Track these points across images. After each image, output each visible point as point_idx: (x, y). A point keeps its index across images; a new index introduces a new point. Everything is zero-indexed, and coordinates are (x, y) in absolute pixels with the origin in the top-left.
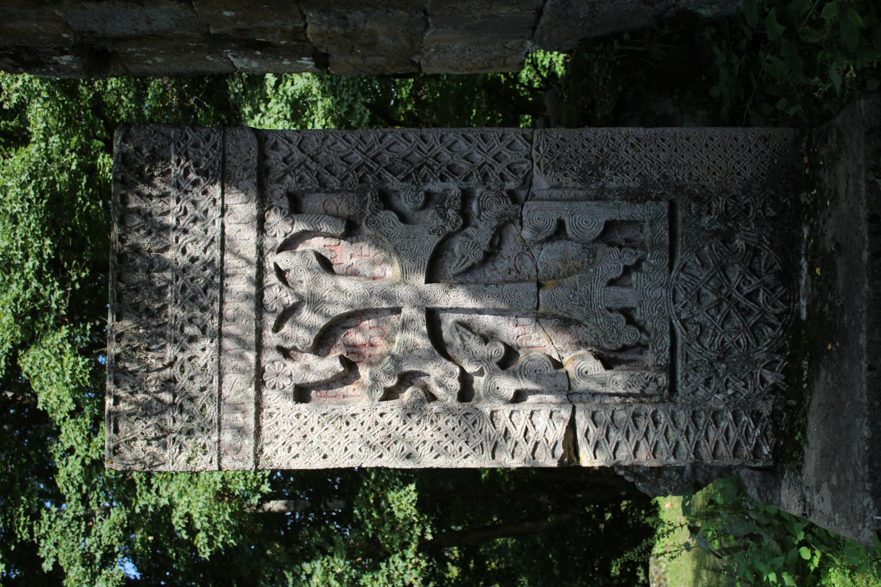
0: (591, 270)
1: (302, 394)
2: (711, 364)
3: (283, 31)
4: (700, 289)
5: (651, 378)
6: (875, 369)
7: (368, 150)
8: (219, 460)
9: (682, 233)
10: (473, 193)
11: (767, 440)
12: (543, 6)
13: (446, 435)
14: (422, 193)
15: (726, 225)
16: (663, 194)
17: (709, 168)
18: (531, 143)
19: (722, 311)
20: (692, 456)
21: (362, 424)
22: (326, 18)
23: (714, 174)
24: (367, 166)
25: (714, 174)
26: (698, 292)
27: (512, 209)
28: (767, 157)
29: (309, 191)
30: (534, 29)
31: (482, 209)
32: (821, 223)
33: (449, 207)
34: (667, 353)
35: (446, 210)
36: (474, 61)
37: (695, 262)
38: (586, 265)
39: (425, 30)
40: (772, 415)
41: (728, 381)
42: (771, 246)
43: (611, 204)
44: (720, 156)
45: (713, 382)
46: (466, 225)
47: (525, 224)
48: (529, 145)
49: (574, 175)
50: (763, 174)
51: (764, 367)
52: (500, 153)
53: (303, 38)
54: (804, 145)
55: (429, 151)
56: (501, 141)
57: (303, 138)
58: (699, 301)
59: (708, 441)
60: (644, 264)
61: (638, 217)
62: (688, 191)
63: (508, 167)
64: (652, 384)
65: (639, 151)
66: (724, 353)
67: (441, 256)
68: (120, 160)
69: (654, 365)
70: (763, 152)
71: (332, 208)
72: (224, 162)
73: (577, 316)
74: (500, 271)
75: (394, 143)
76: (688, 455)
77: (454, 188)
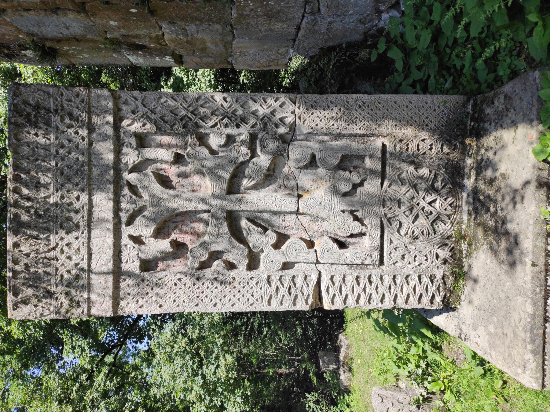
3: (150, 38)
6: (537, 265)
7: (189, 107)
11: (439, 293)
12: (301, 23)
13: (239, 291)
14: (224, 135)
17: (408, 122)
21: (185, 285)
22: (173, 28)
24: (188, 117)
28: (445, 114)
30: (294, 40)
39: (233, 40)
41: (416, 256)
44: (415, 114)
48: (294, 105)
50: (442, 126)
53: (163, 43)
54: (470, 107)
55: (229, 108)
57: (145, 97)
64: (369, 258)
68: (12, 108)
70: (443, 111)
73: (322, 215)
76: (390, 302)
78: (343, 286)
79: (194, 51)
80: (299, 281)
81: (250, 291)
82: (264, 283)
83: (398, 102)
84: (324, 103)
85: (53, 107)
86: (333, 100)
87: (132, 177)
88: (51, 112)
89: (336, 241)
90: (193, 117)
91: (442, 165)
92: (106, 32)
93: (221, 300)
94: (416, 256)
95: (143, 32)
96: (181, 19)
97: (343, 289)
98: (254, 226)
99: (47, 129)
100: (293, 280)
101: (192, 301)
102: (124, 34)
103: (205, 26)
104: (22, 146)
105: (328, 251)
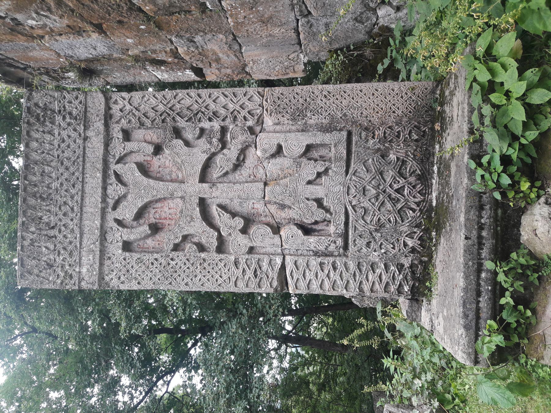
0: (297, 175)
1: (127, 246)
3: (166, 52)
4: (365, 186)
5: (332, 241)
7: (168, 103)
8: (80, 283)
9: (355, 151)
10: (229, 129)
15: (384, 145)
16: (344, 127)
17: (374, 109)
18: (263, 97)
19: (379, 200)
20: (358, 290)
23: (377, 112)
24: (167, 113)
25: (377, 112)
26: (364, 189)
27: (251, 138)
30: (300, 44)
31: (233, 138)
32: (444, 141)
33: (213, 137)
34: (342, 225)
35: (211, 138)
37: (362, 169)
38: (295, 172)
40: (412, 266)
41: (381, 244)
42: (414, 159)
43: (310, 134)
45: (372, 244)
46: (224, 147)
47: (258, 147)
48: (261, 98)
49: (288, 116)
50: (410, 112)
51: (406, 236)
52: (244, 103)
54: (438, 92)
55: (202, 103)
56: (245, 95)
57: (131, 97)
58: (364, 194)
59: (368, 281)
60: (330, 171)
61: (327, 141)
62: (360, 124)
63: (249, 112)
65: (329, 99)
66: (380, 226)
67: (210, 167)
69: (334, 233)
70: (410, 97)
71: (148, 138)
72: (86, 111)
73: (287, 202)
74: (244, 176)
75: (183, 99)
76: (355, 289)
77: (216, 125)
78: (307, 271)
79: (210, 63)
80: (265, 265)
83: (364, 90)
84: (290, 95)
85: (57, 109)
86: (299, 91)
87: (119, 168)
88: (55, 112)
90: (171, 113)
91: (410, 152)
92: (128, 50)
93: (192, 279)
94: (381, 244)
95: (159, 48)
96: (186, 32)
97: (307, 273)
98: (223, 212)
99: (52, 127)
100: (258, 263)
101: (167, 279)
102: (142, 50)
103: (209, 36)
104: (32, 141)
105: (292, 237)
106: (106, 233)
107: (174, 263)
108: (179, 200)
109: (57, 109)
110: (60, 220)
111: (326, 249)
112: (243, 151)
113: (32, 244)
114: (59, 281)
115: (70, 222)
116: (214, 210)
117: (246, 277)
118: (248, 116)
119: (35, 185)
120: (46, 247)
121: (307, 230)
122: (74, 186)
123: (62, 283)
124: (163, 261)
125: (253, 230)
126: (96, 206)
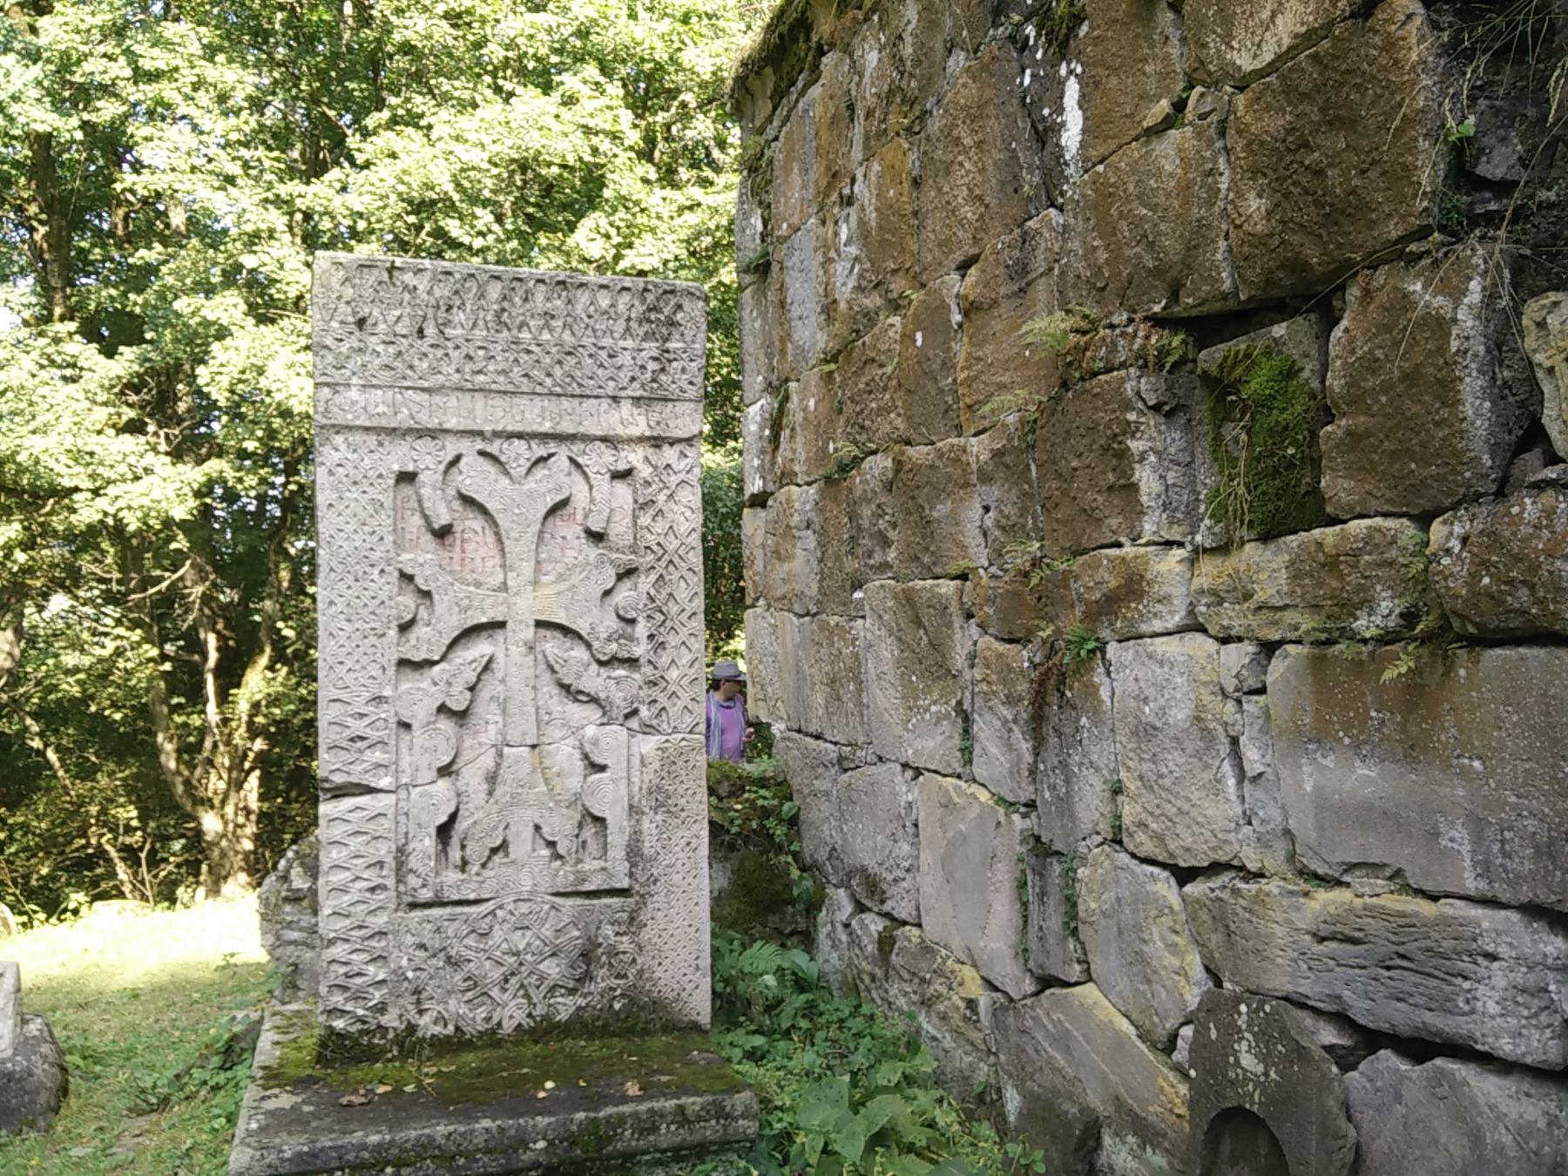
2: (444, 949)
8: (328, 385)
20: (332, 935)
22: (808, 507)
26: (527, 928)
29: (635, 492)
30: (799, 731)
31: (618, 680)
36: (761, 667)
42: (579, 1008)
45: (421, 954)
46: (601, 663)
60: (559, 863)
64: (420, 881)
72: (666, 400)
73: (498, 793)
77: (640, 650)
78: (364, 838)
80: (378, 755)
81: (358, 667)
82: (377, 692)
85: (671, 345)
86: (698, 797)
87: (561, 461)
89: (453, 818)
90: (663, 563)
106: (433, 438)
107: (375, 576)
108: (500, 577)
109: (671, 345)
110: (457, 347)
111: (411, 871)
112: (594, 700)
113: (406, 288)
114: (329, 341)
115: (454, 367)
116: (481, 648)
117: (350, 721)
118: (659, 706)
119: (526, 300)
120: (399, 318)
121: (444, 831)
122: (526, 375)
123: (326, 347)
124: (379, 554)
125: (445, 724)
126: (486, 420)
